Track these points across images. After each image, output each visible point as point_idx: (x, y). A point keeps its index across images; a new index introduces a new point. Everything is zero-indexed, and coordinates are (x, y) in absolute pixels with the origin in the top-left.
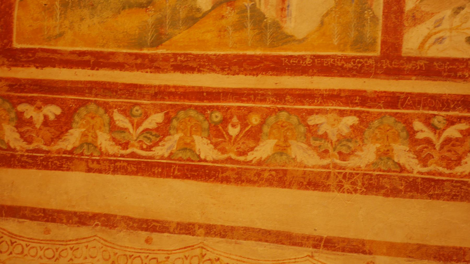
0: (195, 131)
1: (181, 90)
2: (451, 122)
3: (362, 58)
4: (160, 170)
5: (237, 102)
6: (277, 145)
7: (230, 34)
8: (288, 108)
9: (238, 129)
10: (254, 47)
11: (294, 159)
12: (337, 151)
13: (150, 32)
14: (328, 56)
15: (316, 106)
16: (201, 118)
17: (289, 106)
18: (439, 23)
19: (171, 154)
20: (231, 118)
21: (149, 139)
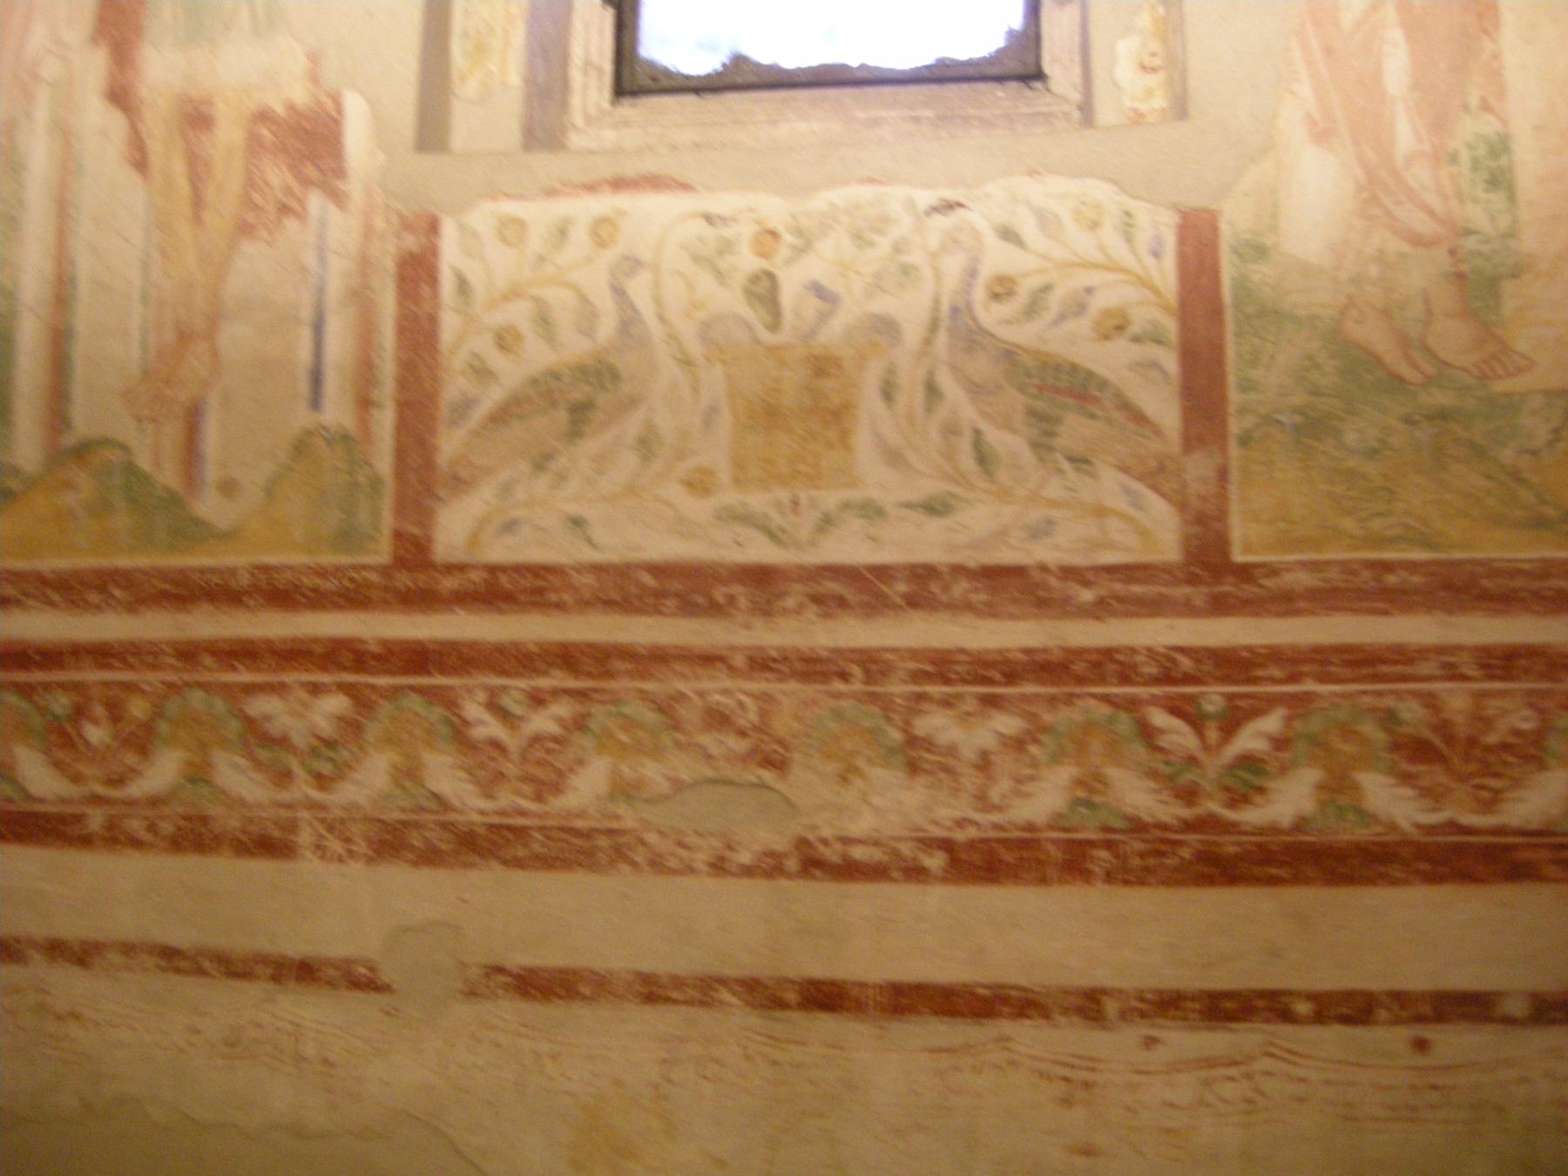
2: (538, 700)
3: (354, 567)
18: (507, 489)
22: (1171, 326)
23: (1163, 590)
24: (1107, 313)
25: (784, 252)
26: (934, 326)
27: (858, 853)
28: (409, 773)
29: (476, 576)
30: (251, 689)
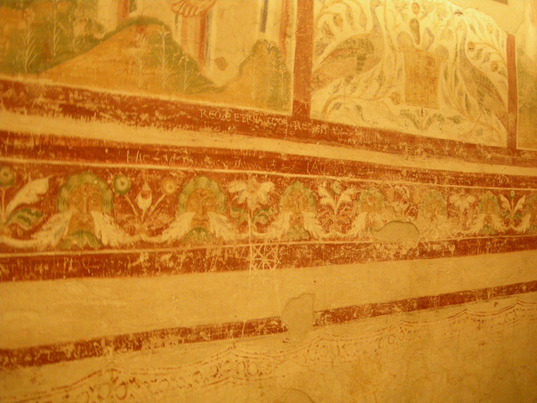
0: (93, 204)
1: (73, 143)
2: (344, 187)
3: (278, 117)
4: (47, 268)
5: (148, 163)
6: (194, 219)
7: (140, 69)
8: (208, 173)
9: (149, 200)
10: (168, 91)
11: (213, 235)
12: (255, 222)
13: (28, 49)
14: (246, 112)
15: (236, 169)
16: (103, 185)
17: (208, 170)
18: (337, 88)
19: (62, 240)
20: (141, 185)
21: (26, 220)
22: (506, 70)
23: (503, 156)
24: (493, 62)
25: (420, 15)
26: (456, 56)
27: (435, 247)
28: (297, 221)
29: (325, 127)
30: (230, 178)
